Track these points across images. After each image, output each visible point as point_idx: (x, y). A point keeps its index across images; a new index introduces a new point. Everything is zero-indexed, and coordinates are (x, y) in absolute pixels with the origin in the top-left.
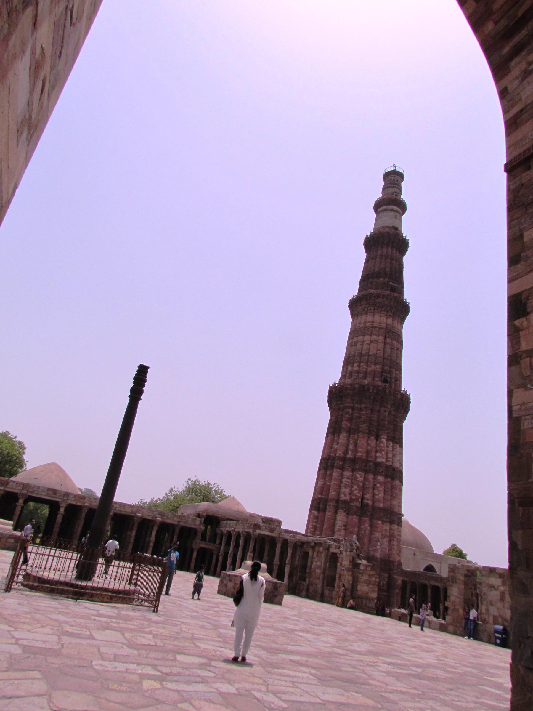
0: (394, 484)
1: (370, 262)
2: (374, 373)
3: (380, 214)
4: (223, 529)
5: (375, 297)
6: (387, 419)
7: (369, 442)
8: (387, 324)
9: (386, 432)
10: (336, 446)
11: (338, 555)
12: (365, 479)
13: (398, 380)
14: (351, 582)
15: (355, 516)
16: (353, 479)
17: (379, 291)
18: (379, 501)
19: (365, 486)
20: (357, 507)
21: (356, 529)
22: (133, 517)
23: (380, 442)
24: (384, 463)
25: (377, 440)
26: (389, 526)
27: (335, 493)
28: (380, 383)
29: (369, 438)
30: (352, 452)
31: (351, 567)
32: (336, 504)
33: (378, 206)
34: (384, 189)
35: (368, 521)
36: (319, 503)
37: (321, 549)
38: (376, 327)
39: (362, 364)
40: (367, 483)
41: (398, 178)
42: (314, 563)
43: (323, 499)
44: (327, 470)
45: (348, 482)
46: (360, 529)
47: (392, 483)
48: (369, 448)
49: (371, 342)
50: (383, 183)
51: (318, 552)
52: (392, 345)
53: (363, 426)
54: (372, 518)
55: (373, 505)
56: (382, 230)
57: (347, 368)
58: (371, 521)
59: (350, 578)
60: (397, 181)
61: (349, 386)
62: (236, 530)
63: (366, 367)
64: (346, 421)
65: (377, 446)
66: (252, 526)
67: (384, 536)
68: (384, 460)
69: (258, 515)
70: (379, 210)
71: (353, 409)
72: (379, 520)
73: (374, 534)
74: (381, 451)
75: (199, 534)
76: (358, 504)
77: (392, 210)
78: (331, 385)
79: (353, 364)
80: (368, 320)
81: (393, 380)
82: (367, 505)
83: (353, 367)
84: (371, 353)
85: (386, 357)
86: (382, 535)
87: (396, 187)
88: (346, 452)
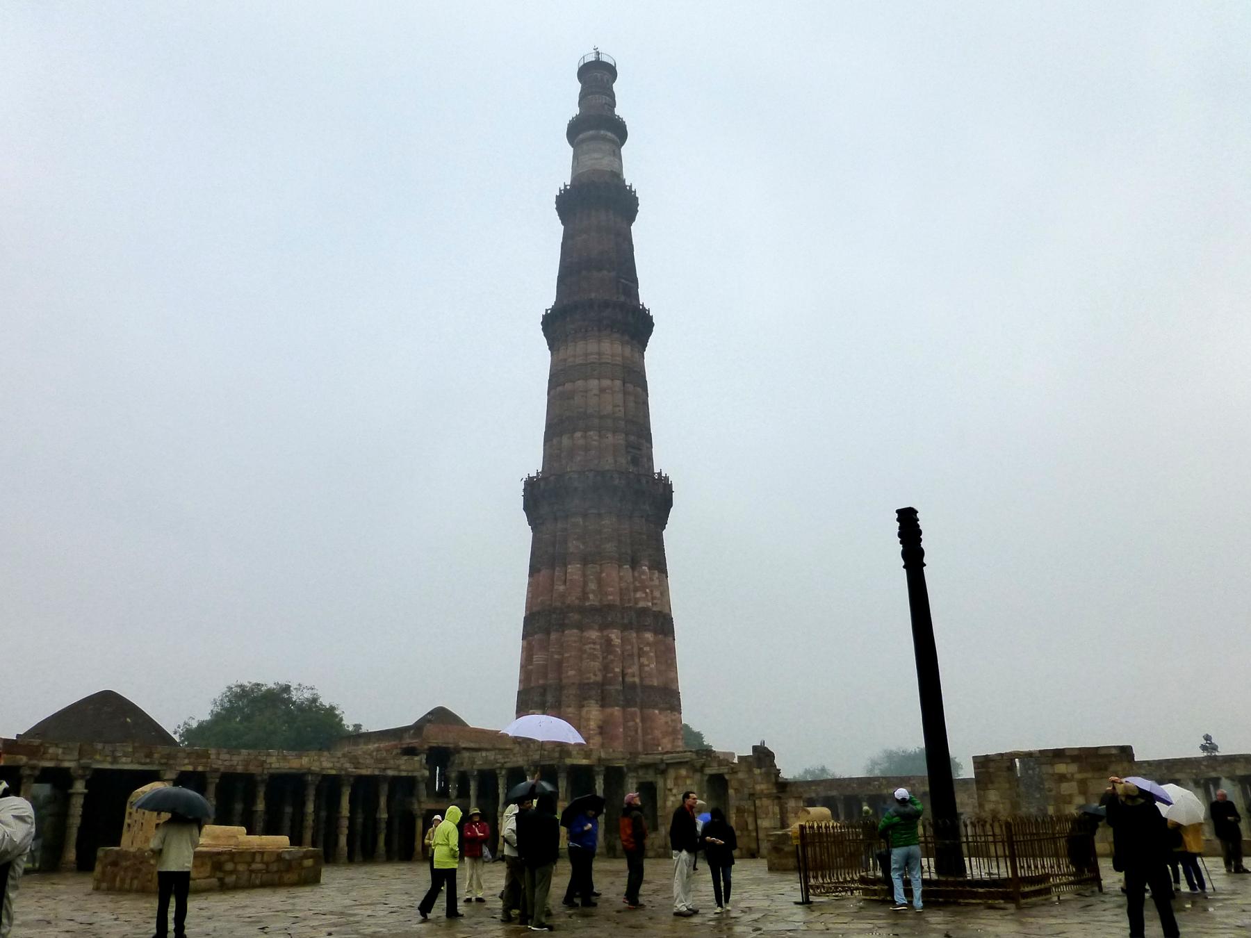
4: (465, 768)
8: (623, 357)
10: (562, 588)
11: (727, 777)
13: (650, 459)
22: (304, 774)
25: (633, 568)
29: (620, 566)
33: (575, 131)
39: (591, 433)
44: (548, 633)
48: (623, 585)
49: (602, 390)
51: (676, 779)
53: (610, 547)
54: (643, 707)
57: (561, 443)
59: (777, 809)
62: (509, 765)
67: (665, 734)
70: (581, 136)
71: (585, 516)
74: (643, 588)
75: (422, 787)
76: (620, 687)
78: (534, 474)
82: (634, 683)
88: (584, 596)
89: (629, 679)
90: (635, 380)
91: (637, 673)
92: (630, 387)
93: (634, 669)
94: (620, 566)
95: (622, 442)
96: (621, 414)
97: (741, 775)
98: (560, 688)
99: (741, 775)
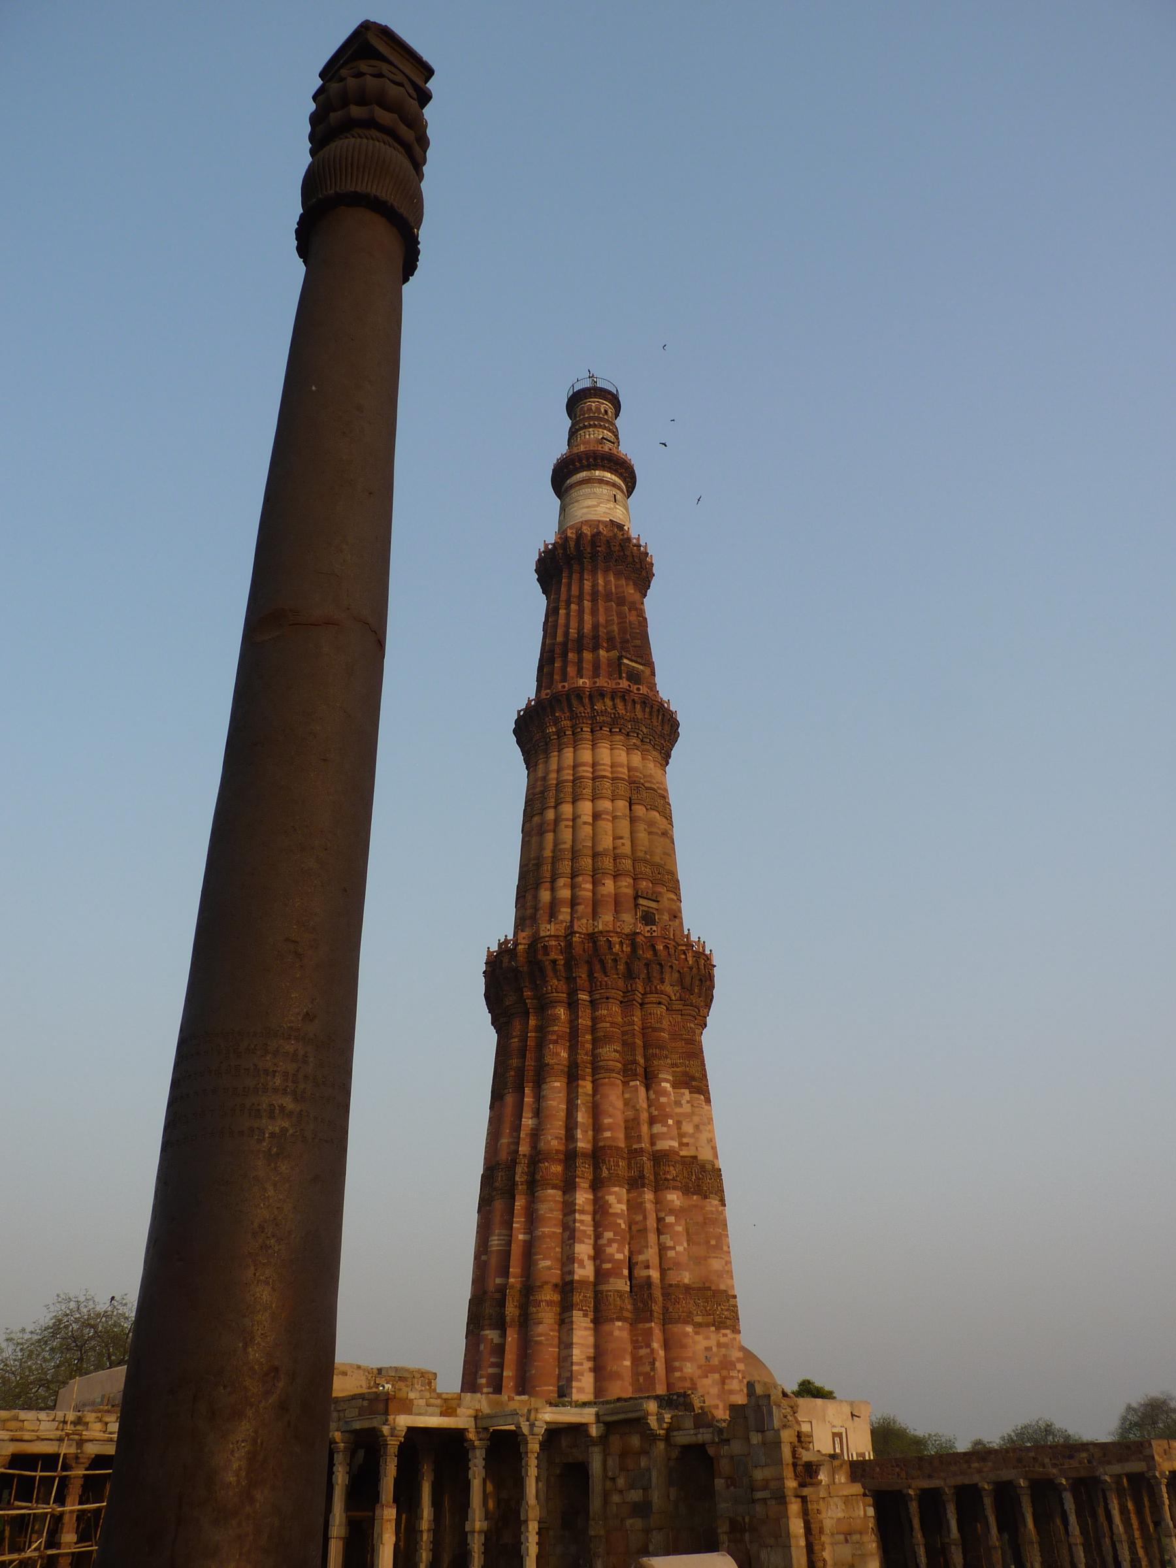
0: (709, 1208)
1: (562, 612)
2: (617, 900)
3: (574, 493)
5: (591, 697)
6: (665, 1024)
7: (627, 1096)
9: (669, 1061)
11: (711, 1451)
12: (635, 1206)
13: (676, 915)
14: (803, 1543)
15: (619, 1324)
16: (600, 1210)
17: (602, 682)
18: (677, 1265)
19: (634, 1228)
20: (620, 1294)
21: (628, 1363)
23: (655, 1092)
24: (677, 1153)
25: (648, 1088)
26: (713, 1336)
27: (548, 1263)
28: (640, 927)
30: (585, 1132)
31: (791, 1484)
32: (556, 1297)
33: (564, 477)
34: (573, 433)
35: (657, 1333)
36: (502, 1304)
37: (635, 1441)
38: (604, 777)
39: (580, 879)
40: (639, 1218)
41: (606, 405)
42: (616, 1498)
43: (512, 1287)
44: (513, 1198)
45: (582, 1222)
46: (636, 1360)
47: (702, 1208)
48: (630, 1114)
50: (568, 423)
51: (624, 1454)
52: (651, 824)
54: (667, 1321)
55: (662, 1279)
56: (586, 530)
57: (536, 897)
58: (664, 1331)
60: (606, 412)
61: (553, 943)
63: (589, 886)
64: (556, 1042)
65: (649, 1106)
66: (381, 1406)
67: (708, 1370)
68: (675, 1144)
69: (359, 1367)
71: (572, 1005)
72: (686, 1322)
73: (681, 1370)
77: (601, 481)
78: (494, 948)
79: (553, 881)
80: (580, 760)
81: (666, 917)
82: (648, 1282)
83: (553, 890)
84: (600, 849)
85: (640, 854)
86: (700, 1367)
87: (605, 428)
89: (640, 1273)
90: (648, 799)
91: (655, 1261)
92: (640, 810)
93: (651, 1254)
94: (625, 1083)
95: (630, 891)
96: (627, 849)
97: (736, 1447)
98: (528, 1290)
99: (736, 1447)
